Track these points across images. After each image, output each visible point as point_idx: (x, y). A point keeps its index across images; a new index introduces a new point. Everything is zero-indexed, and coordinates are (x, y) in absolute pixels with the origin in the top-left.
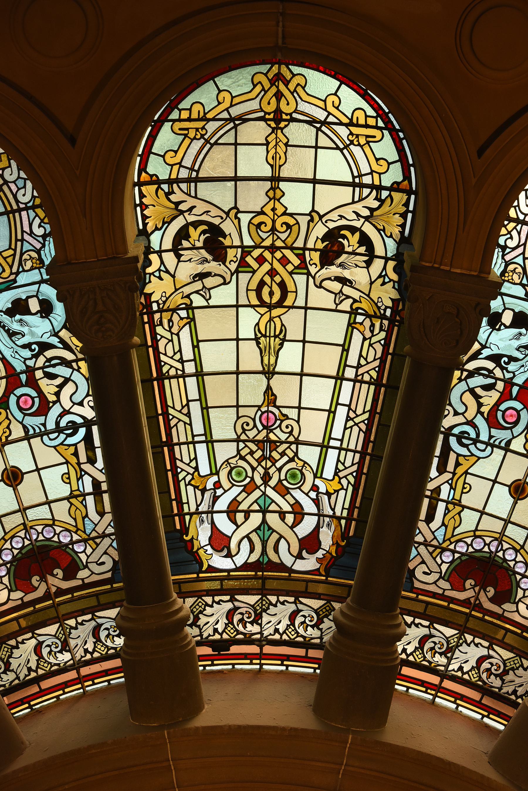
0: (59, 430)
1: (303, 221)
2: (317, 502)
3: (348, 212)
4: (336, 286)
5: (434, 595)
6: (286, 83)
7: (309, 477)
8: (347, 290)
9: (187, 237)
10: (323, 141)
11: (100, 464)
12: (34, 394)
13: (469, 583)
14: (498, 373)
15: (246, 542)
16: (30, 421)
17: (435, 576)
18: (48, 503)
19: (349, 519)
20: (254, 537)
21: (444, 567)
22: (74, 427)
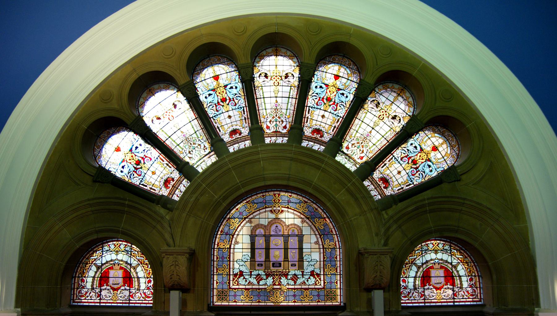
1: (282, 72)
2: (286, 120)
4: (288, 82)
5: (309, 136)
7: (284, 115)
8: (290, 83)
14: (317, 96)
17: (308, 133)
19: (292, 122)
20: (274, 126)
22: (241, 108)
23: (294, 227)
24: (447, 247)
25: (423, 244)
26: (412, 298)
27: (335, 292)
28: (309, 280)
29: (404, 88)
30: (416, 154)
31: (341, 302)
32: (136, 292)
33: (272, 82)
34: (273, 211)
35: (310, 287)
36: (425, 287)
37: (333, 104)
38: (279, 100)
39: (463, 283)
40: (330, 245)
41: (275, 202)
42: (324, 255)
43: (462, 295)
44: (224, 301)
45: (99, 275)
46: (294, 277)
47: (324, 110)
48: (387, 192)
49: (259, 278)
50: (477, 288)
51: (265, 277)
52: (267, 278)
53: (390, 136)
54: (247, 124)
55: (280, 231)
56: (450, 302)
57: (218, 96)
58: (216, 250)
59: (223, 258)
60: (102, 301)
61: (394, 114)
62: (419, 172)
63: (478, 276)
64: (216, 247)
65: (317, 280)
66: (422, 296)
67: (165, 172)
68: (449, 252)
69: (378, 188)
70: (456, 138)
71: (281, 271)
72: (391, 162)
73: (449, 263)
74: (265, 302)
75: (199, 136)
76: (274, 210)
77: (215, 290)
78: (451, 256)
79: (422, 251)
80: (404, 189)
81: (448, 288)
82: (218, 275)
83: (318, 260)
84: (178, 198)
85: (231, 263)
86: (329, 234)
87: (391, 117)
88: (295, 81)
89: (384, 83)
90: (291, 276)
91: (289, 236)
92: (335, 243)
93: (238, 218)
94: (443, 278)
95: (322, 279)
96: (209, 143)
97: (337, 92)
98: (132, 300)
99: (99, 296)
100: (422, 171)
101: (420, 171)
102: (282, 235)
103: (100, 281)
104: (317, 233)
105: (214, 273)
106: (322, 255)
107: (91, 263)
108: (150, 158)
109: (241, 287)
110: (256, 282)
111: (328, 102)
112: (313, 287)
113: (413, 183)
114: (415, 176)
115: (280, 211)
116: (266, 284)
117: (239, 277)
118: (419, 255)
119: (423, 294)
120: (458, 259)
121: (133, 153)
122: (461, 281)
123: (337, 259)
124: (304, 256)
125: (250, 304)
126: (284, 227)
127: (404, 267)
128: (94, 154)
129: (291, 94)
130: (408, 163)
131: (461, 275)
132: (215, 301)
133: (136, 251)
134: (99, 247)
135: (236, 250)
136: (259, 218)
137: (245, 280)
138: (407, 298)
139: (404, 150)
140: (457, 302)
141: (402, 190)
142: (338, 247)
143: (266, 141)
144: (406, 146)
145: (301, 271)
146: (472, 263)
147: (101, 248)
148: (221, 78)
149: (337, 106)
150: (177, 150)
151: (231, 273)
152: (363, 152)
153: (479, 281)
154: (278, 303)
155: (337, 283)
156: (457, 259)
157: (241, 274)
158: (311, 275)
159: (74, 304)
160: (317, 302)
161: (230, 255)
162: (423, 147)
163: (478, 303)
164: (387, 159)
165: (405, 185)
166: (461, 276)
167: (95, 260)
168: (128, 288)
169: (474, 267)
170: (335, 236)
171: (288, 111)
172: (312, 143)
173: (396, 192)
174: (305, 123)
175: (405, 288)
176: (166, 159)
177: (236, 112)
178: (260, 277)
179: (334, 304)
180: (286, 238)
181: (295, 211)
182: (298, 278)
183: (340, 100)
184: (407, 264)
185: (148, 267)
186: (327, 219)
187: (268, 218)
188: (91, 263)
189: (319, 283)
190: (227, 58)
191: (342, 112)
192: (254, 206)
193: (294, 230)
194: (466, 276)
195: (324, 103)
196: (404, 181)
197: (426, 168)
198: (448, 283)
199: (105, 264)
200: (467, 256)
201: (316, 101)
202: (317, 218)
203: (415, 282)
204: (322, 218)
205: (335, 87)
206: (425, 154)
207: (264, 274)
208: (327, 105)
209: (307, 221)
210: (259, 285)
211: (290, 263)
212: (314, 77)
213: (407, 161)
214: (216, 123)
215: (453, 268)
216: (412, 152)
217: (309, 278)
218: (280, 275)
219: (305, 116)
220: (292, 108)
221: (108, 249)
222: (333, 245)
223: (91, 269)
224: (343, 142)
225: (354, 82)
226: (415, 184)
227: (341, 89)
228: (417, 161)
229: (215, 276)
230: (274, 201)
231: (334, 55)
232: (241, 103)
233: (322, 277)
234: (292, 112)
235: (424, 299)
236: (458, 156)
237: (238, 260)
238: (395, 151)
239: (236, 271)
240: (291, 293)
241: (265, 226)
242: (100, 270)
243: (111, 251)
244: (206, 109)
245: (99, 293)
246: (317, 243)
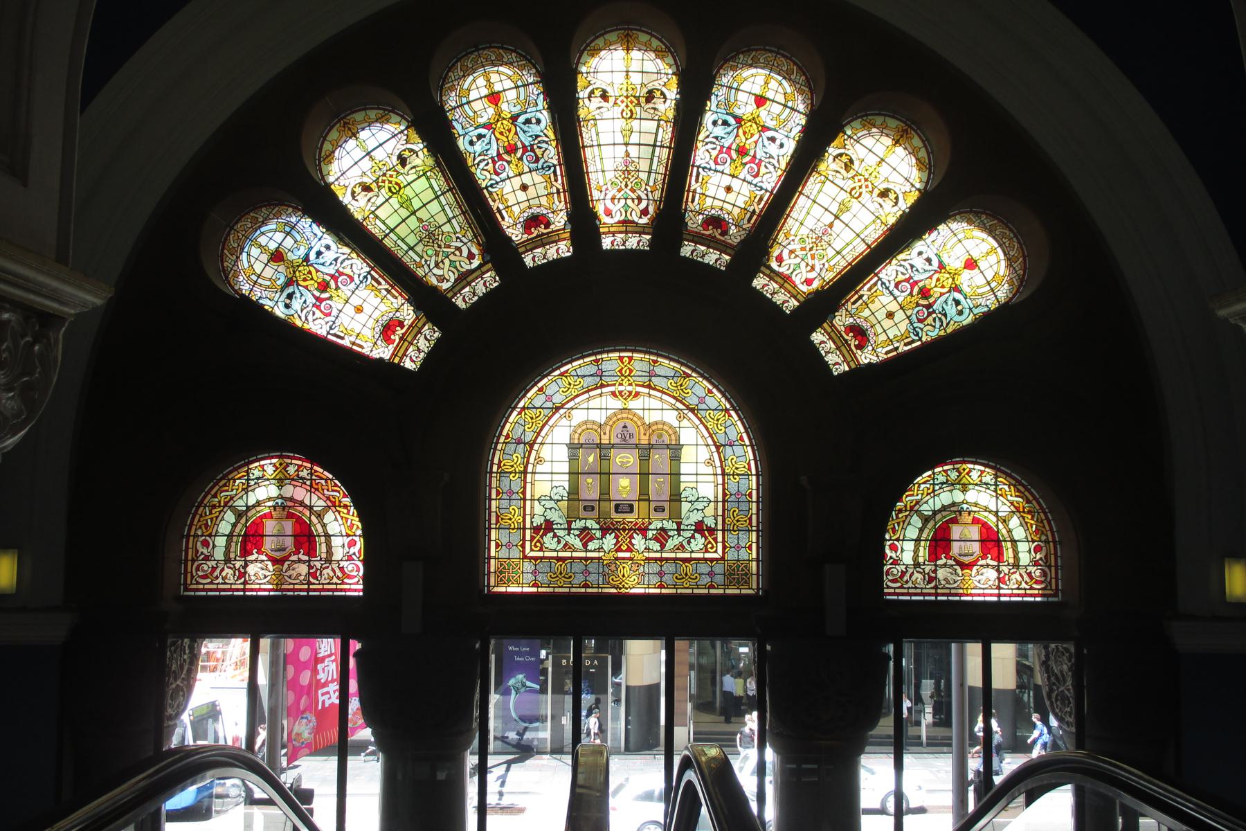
0: (543, 168)
1: (639, 87)
2: (647, 195)
3: (656, 83)
4: (652, 111)
5: (696, 232)
6: (631, 37)
9: (593, 93)
10: (645, 57)
11: (560, 181)
12: (533, 154)
13: (710, 227)
14: (717, 142)
15: (619, 213)
16: (531, 165)
17: (696, 225)
18: (538, 197)
19: (660, 201)
21: (700, 221)
22: (549, 167)
23: (662, 429)
24: (988, 478)
25: (936, 470)
26: (910, 585)
27: (746, 567)
28: (692, 540)
29: (910, 126)
30: (929, 274)
31: (758, 589)
32: (324, 566)
33: (617, 110)
34: (617, 394)
35: (694, 555)
36: (939, 562)
37: (750, 162)
38: (633, 151)
39: (1020, 555)
40: (737, 468)
41: (622, 375)
42: (724, 489)
43: (1017, 581)
44: (513, 583)
45: (241, 531)
46: (660, 534)
47: (730, 175)
48: (863, 356)
49: (586, 535)
50: (1049, 567)
51: (598, 534)
52: (603, 536)
53: (874, 234)
54: (563, 203)
55: (631, 436)
56: (991, 595)
57: (497, 140)
58: (494, 475)
59: (511, 492)
60: (248, 586)
61: (885, 185)
62: (934, 315)
63: (1054, 541)
64: (495, 468)
65: (710, 542)
66: (931, 580)
67: (383, 308)
68: (992, 488)
69: (843, 348)
70: (1019, 242)
71: (632, 522)
72: (872, 291)
73: (990, 512)
74: (598, 587)
75: (458, 229)
76: (620, 392)
77: (492, 561)
78: (997, 498)
79: (934, 484)
80: (900, 350)
81: (988, 565)
82: (499, 528)
83: (712, 500)
84: (412, 364)
85: (528, 503)
86: (736, 443)
87: (876, 192)
88: (667, 108)
89: (867, 115)
90: (655, 532)
91: (650, 446)
92: (749, 464)
93: (543, 408)
94: (977, 543)
95: (720, 539)
96: (479, 244)
97: (761, 136)
98: (314, 584)
99: (242, 575)
100: (940, 313)
101: (937, 312)
102: (637, 446)
103: (244, 543)
104: (710, 442)
105: (490, 524)
106: (720, 487)
107: (222, 504)
108: (349, 276)
109: (547, 554)
110: (580, 544)
111: (740, 157)
112: (700, 555)
113: (920, 339)
114: (926, 323)
115: (633, 394)
116: (602, 548)
117: (545, 534)
118: (928, 494)
119: (933, 575)
120: (1012, 504)
121: (312, 265)
122: (1016, 552)
123: (751, 498)
124: (682, 490)
125: (567, 590)
126: (641, 427)
127: (895, 518)
128: (223, 267)
129: (659, 139)
130: (911, 294)
131: (1016, 538)
132: (492, 583)
133: (322, 479)
134: (240, 471)
135: (537, 477)
136: (588, 409)
137: (556, 539)
138: (899, 585)
139: (904, 266)
140: (1005, 595)
141: (895, 353)
142: (754, 472)
143: (603, 241)
144: (908, 257)
145: (676, 523)
146: (1042, 514)
147: (245, 474)
148: (505, 100)
149: (759, 165)
150: (410, 259)
151: (528, 525)
152: (813, 268)
153: (1056, 554)
154: (627, 589)
155: (750, 548)
156: (1009, 505)
157: (548, 526)
158: (695, 531)
159: (186, 593)
160: (709, 588)
161: (525, 487)
162: (945, 260)
163: (1051, 599)
164: (865, 285)
165: (903, 343)
166: (1016, 541)
167: (232, 498)
168: (306, 558)
169: (1045, 522)
170: (749, 448)
171: (653, 175)
172: (703, 248)
173: (883, 357)
174: (690, 204)
175: (895, 562)
176: (384, 279)
177: (538, 178)
178: (588, 533)
179: (743, 592)
180: (645, 452)
181: (665, 393)
182: (669, 536)
183: (766, 153)
184: (900, 511)
185: (348, 513)
186: (733, 413)
187: (607, 409)
188: (222, 504)
189: (712, 548)
190: (517, 53)
191: (769, 180)
192: (578, 383)
193: (661, 435)
194: (1028, 541)
195: (731, 158)
196: (899, 334)
197: (949, 307)
198: (989, 555)
199: (254, 506)
200: (1031, 498)
201: (714, 153)
202: (710, 409)
203: (916, 551)
204: (722, 410)
205: (756, 123)
206: (948, 276)
207: (598, 527)
208: (738, 163)
209: (690, 415)
210: (586, 551)
211: (653, 505)
212: (710, 101)
213: (909, 291)
214: (494, 201)
215: (1000, 523)
216: (921, 271)
217: (693, 537)
218: (630, 530)
219: (689, 186)
220: (662, 170)
221: (261, 474)
222: (744, 467)
223: (223, 519)
224: (771, 247)
225: (799, 112)
226: (924, 339)
227: (769, 129)
228: (929, 290)
229: (493, 532)
230: (620, 371)
231: (756, 50)
232: (550, 156)
233: (720, 535)
234: (660, 177)
235: (936, 587)
236: (1022, 282)
237: (543, 498)
238: (883, 268)
239: (538, 521)
240: (655, 568)
241: (600, 426)
242: (243, 521)
243: (268, 480)
244: (473, 169)
245: (242, 571)
246: (710, 462)
